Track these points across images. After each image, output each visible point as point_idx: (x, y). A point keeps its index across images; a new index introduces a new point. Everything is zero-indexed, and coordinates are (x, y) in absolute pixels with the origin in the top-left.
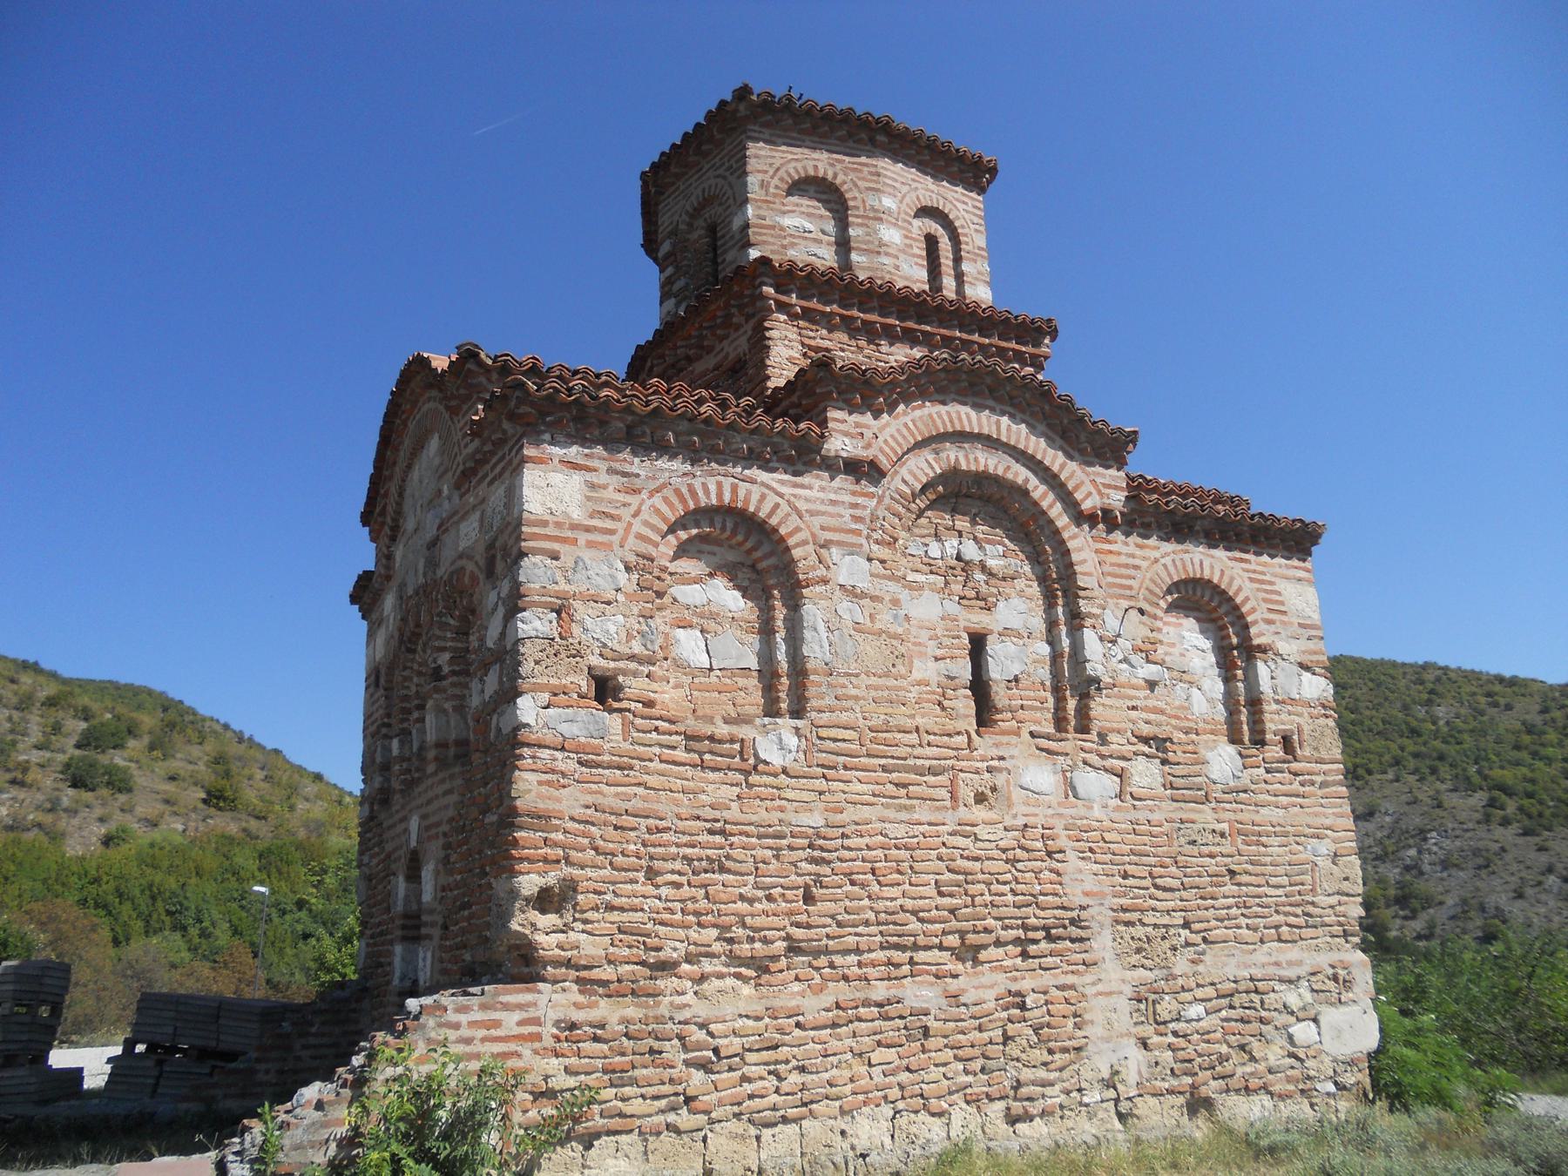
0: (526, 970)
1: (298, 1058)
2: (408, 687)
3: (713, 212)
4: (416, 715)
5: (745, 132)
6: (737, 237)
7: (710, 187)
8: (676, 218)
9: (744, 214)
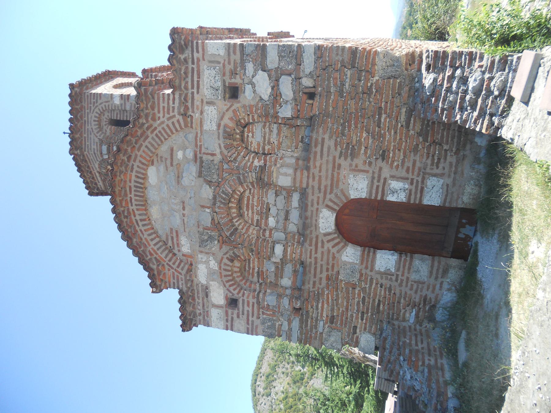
0: (416, 62)
1: (423, 348)
2: (252, 238)
3: (105, 120)
4: (267, 233)
5: (85, 93)
6: (123, 102)
7: (95, 117)
8: (97, 140)
9: (116, 96)
